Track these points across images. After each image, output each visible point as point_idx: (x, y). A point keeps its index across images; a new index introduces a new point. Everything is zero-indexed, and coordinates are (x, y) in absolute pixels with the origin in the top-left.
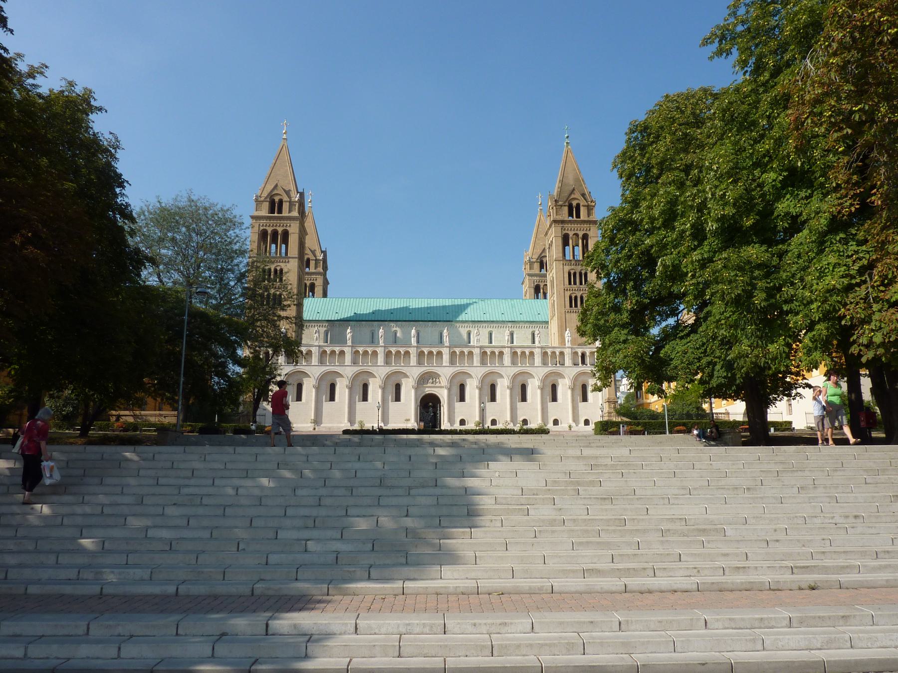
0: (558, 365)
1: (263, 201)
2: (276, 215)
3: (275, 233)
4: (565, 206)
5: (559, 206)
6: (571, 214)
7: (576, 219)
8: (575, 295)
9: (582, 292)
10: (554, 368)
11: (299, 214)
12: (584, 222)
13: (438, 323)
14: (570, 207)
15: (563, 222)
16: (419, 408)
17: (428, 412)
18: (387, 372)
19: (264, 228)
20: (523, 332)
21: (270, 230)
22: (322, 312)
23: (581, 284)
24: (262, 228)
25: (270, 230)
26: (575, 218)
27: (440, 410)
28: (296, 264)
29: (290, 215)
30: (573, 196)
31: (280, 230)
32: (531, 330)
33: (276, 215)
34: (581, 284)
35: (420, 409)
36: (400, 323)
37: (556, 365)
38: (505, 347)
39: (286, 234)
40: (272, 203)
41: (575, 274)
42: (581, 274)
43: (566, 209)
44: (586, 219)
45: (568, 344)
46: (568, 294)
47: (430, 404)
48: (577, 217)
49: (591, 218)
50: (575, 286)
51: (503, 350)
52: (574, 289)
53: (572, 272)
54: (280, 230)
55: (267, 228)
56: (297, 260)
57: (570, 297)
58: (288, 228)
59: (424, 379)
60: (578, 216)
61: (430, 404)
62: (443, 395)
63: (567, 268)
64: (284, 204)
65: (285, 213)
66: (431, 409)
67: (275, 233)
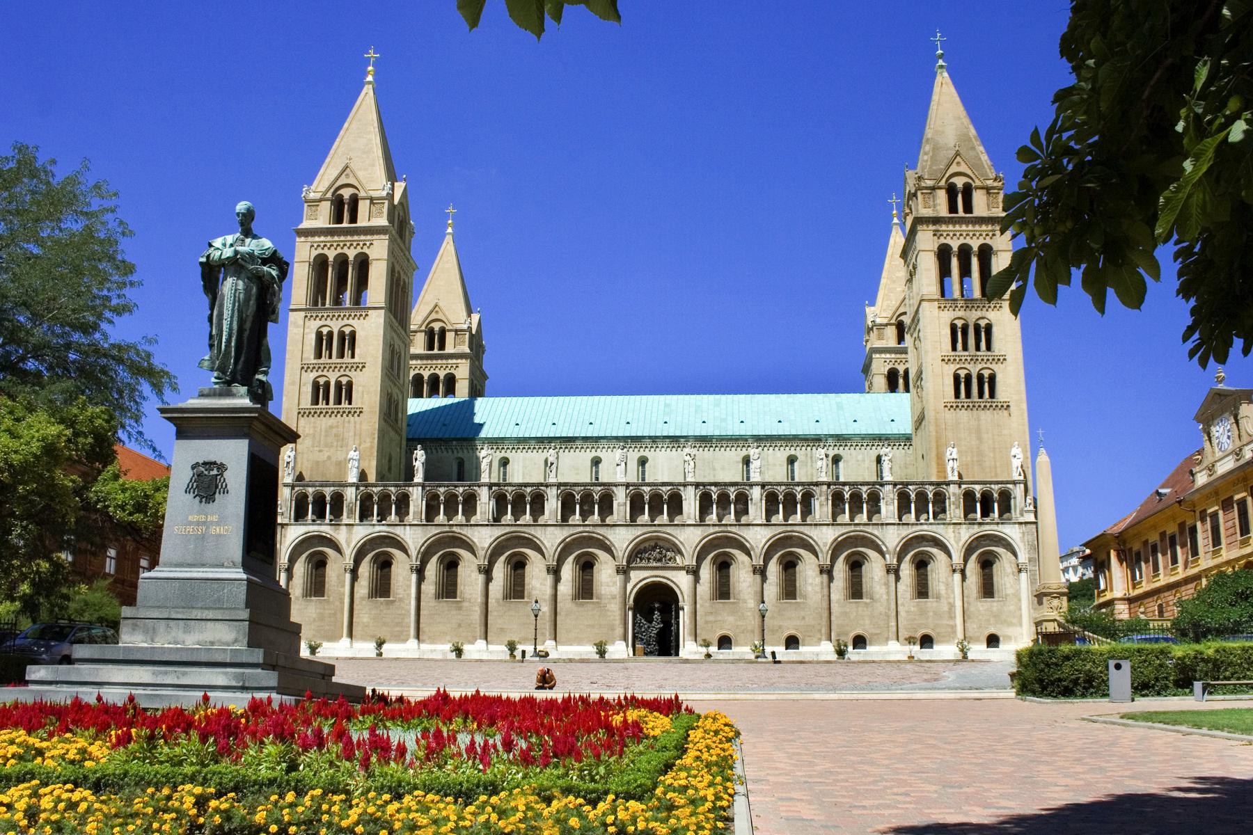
1: (320, 200)
2: (345, 225)
3: (342, 261)
4: (940, 188)
5: (926, 188)
6: (953, 208)
7: (963, 215)
8: (966, 372)
9: (980, 366)
11: (390, 222)
14: (951, 191)
15: (936, 221)
16: (630, 613)
17: (650, 622)
18: (563, 538)
19: (322, 252)
20: (860, 457)
21: (331, 255)
23: (978, 348)
25: (331, 255)
26: (961, 213)
27: (677, 617)
28: (382, 320)
31: (351, 254)
32: (874, 453)
33: (345, 225)
34: (978, 348)
39: (363, 263)
40: (338, 203)
41: (965, 329)
42: (977, 328)
43: (942, 196)
44: (985, 214)
46: (952, 368)
47: (657, 605)
50: (966, 353)
52: (963, 358)
53: (959, 323)
55: (326, 251)
56: (383, 312)
57: (957, 378)
58: (365, 250)
59: (639, 553)
60: (968, 208)
62: (681, 581)
63: (947, 316)
64: (361, 203)
65: (362, 222)
66: (657, 615)
67: (342, 261)
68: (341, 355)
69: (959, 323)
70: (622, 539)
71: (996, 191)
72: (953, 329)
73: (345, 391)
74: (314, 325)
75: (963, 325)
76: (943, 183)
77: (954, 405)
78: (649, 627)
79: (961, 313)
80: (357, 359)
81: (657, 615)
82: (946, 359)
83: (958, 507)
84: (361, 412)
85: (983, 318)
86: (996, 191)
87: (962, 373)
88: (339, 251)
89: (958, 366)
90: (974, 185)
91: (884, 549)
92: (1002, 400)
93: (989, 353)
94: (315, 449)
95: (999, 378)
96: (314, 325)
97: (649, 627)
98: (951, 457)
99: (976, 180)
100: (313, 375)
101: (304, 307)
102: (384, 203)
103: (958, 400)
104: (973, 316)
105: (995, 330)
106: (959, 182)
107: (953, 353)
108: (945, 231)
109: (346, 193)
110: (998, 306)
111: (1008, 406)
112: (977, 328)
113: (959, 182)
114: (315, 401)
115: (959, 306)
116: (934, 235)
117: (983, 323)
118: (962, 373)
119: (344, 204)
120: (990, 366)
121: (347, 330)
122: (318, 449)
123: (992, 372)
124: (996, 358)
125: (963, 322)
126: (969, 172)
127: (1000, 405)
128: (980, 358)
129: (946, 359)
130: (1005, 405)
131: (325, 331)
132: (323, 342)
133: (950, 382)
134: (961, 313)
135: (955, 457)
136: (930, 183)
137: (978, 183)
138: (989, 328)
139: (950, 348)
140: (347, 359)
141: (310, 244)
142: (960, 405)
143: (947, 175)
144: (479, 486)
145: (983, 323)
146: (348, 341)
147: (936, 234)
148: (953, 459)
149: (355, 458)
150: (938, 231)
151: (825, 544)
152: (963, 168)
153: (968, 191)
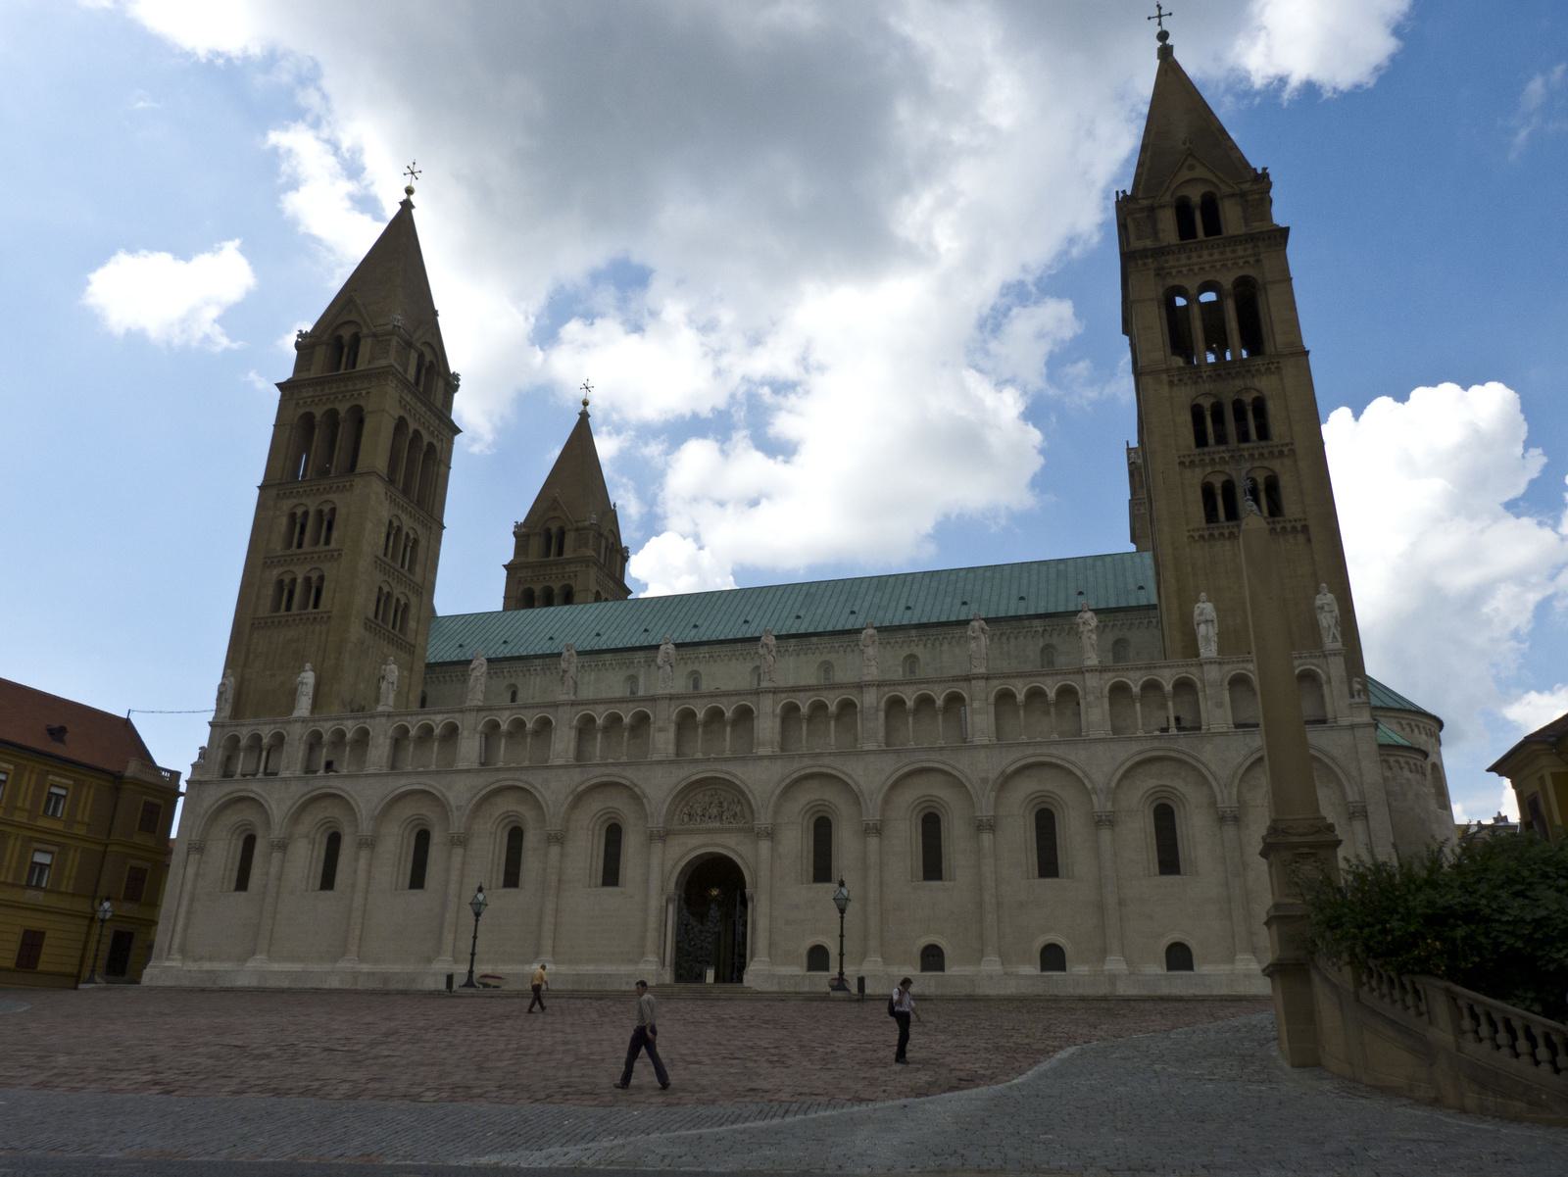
0: (1173, 731)
2: (342, 371)
4: (1162, 207)
5: (1142, 210)
6: (1186, 230)
8: (1223, 478)
9: (1248, 466)
10: (1156, 744)
12: (1235, 240)
13: (814, 640)
14: (1183, 209)
15: (1160, 252)
21: (319, 412)
22: (513, 644)
23: (1244, 437)
24: (301, 411)
25: (319, 412)
29: (370, 367)
30: (1186, 174)
31: (343, 408)
34: (1244, 437)
35: (679, 911)
36: (706, 648)
37: (1165, 730)
38: (968, 679)
40: (338, 345)
42: (1239, 409)
44: (1243, 230)
45: (1209, 650)
46: (1195, 478)
47: (715, 892)
48: (1207, 234)
49: (1257, 226)
51: (961, 688)
52: (1217, 457)
53: (1207, 403)
54: (343, 408)
58: (362, 403)
60: (1213, 226)
61: (715, 892)
65: (361, 365)
66: (714, 912)
68: (316, 542)
69: (1207, 403)
70: (659, 785)
71: (1257, 196)
72: (1197, 414)
73: (315, 591)
74: (287, 505)
75: (1213, 405)
76: (1167, 198)
77: (1206, 534)
78: (701, 932)
79: (1207, 387)
80: (333, 545)
81: (714, 912)
82: (1187, 461)
83: (1220, 705)
84: (329, 617)
85: (1247, 389)
86: (1257, 196)
87: (1218, 482)
88: (330, 406)
89: (1209, 469)
90: (1218, 195)
91: (1089, 786)
92: (1291, 518)
93: (1263, 443)
94: (268, 673)
95: (1286, 482)
96: (287, 505)
97: (701, 932)
98: (1202, 618)
99: (1221, 186)
100: (275, 572)
101: (278, 482)
102: (390, 340)
103: (1212, 525)
104: (1229, 391)
105: (1273, 408)
106: (1195, 195)
107: (1198, 451)
108: (1174, 267)
109: (346, 334)
110: (1273, 367)
111: (1305, 529)
112: (1239, 409)
113: (1195, 195)
114: (277, 608)
115: (1205, 376)
116: (1158, 275)
117: (1248, 398)
118: (1218, 482)
119: (341, 348)
120: (1266, 464)
121: (326, 509)
122: (268, 673)
123: (1270, 473)
124: (1276, 450)
125: (1212, 400)
126: (1209, 176)
127: (1289, 526)
128: (1246, 454)
129: (1187, 461)
130: (1299, 526)
131: (299, 511)
132: (297, 525)
133: (1196, 497)
134: (1207, 387)
135: (1210, 618)
136: (1145, 203)
137: (1225, 189)
138: (1260, 407)
139: (1191, 440)
140: (321, 547)
141: (294, 402)
142: (1216, 533)
143: (1173, 186)
144: (461, 711)
145: (1248, 398)
146: (327, 522)
147: (1160, 273)
148: (1207, 621)
149: (305, 681)
150: (1163, 268)
151: (985, 781)
152: (1200, 172)
153: (1210, 206)
